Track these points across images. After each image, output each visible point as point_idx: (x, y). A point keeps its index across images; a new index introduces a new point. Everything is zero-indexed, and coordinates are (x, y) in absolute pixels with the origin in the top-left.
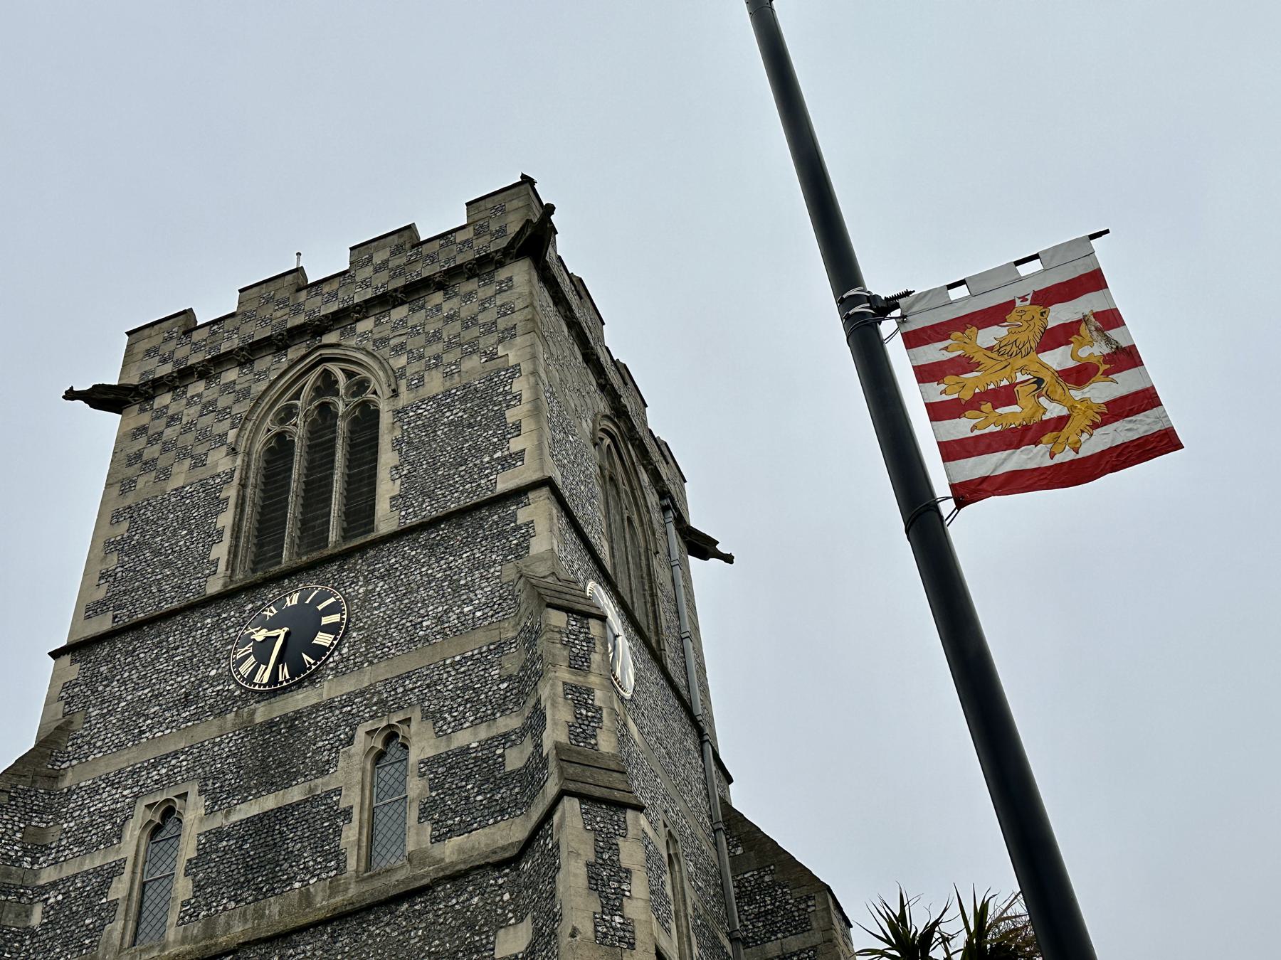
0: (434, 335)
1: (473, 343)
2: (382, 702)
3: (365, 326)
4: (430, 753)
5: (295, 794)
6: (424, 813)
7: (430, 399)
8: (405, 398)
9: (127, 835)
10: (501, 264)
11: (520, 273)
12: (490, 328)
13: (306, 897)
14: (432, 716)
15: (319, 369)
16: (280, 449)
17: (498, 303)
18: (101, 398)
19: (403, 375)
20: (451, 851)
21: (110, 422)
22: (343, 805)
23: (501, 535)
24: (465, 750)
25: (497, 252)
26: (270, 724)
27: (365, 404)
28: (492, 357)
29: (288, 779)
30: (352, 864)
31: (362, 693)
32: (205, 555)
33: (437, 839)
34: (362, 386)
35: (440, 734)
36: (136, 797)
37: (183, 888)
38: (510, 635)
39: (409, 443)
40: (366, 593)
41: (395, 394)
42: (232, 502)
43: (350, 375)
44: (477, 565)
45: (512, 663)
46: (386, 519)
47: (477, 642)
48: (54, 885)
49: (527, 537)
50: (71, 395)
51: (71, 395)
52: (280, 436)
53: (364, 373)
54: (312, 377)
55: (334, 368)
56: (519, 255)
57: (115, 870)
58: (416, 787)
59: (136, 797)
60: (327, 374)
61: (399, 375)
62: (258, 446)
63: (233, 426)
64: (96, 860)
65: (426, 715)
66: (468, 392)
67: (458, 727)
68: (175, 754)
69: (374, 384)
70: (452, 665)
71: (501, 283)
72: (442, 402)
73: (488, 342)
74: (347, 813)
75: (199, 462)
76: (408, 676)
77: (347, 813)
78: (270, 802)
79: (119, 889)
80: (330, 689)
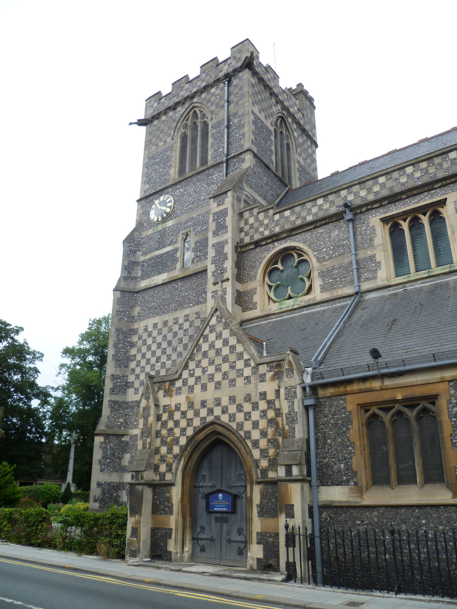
11: (246, 74)
15: (193, 111)
18: (141, 123)
21: (144, 128)
27: (205, 122)
34: (204, 116)
43: (201, 112)
46: (210, 162)
52: (185, 133)
53: (205, 112)
56: (246, 68)
60: (195, 112)
61: (212, 112)
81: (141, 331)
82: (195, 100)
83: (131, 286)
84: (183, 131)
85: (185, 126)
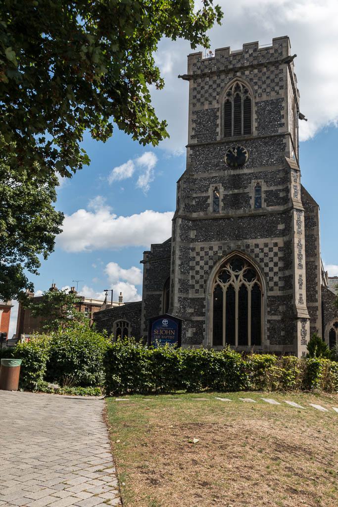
0: (265, 81)
1: (274, 88)
2: (256, 176)
3: (247, 73)
4: (266, 190)
5: (241, 191)
6: (265, 201)
7: (264, 102)
8: (258, 100)
9: (209, 191)
10: (280, 64)
12: (277, 84)
13: (245, 211)
14: (266, 182)
15: (236, 82)
16: (228, 103)
17: (280, 77)
18: (185, 77)
19: (256, 92)
20: (270, 208)
22: (250, 196)
23: (280, 144)
24: (272, 191)
25: (280, 60)
26: (234, 175)
27: (247, 97)
28: (278, 93)
29: (239, 188)
30: (253, 207)
31: (252, 173)
32: (215, 130)
33: (267, 206)
34: (246, 92)
35: (267, 186)
36: (210, 183)
37: (221, 204)
38: (280, 169)
39: (259, 113)
40: (252, 150)
41: (255, 97)
42: (220, 116)
43: (244, 87)
44: (275, 150)
45: (281, 175)
46: (255, 132)
47: (274, 169)
48: (196, 197)
49: (285, 146)
50: (179, 77)
51: (179, 77)
52: (228, 100)
53: (247, 88)
54: (235, 84)
55: (240, 83)
57: (208, 197)
58: (263, 196)
59: (210, 183)
60: (237, 84)
61: (256, 91)
62: (223, 102)
63: (217, 95)
64: (204, 195)
65: (265, 181)
66: (272, 102)
67: (271, 186)
68: (216, 177)
69: (249, 92)
70: (270, 172)
71: (280, 70)
72: (266, 102)
73: (277, 88)
74: (251, 197)
75: (210, 103)
76: (261, 172)
77: (251, 197)
78: (236, 191)
79: (210, 201)
80: (246, 171)
81: (198, 249)
82: (238, 74)
83: (188, 214)
84: (227, 98)
85: (229, 94)
